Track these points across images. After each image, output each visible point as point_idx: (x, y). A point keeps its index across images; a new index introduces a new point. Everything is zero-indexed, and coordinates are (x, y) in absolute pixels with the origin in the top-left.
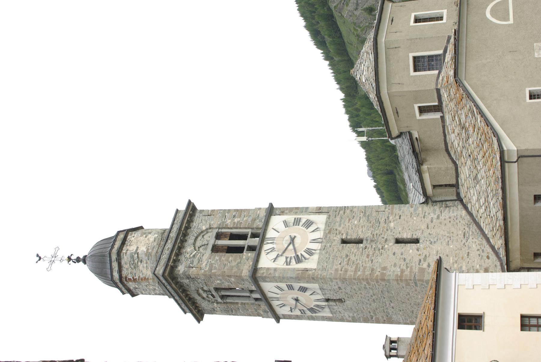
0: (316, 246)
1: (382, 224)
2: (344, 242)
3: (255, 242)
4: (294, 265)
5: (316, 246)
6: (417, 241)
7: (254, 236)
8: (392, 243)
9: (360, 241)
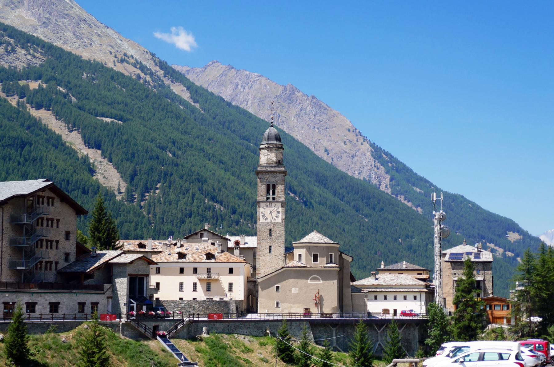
0: (268, 221)
1: (277, 241)
2: (270, 230)
3: (271, 200)
4: (261, 215)
5: (268, 221)
6: (270, 252)
7: (274, 199)
8: (270, 245)
9: (271, 234)
